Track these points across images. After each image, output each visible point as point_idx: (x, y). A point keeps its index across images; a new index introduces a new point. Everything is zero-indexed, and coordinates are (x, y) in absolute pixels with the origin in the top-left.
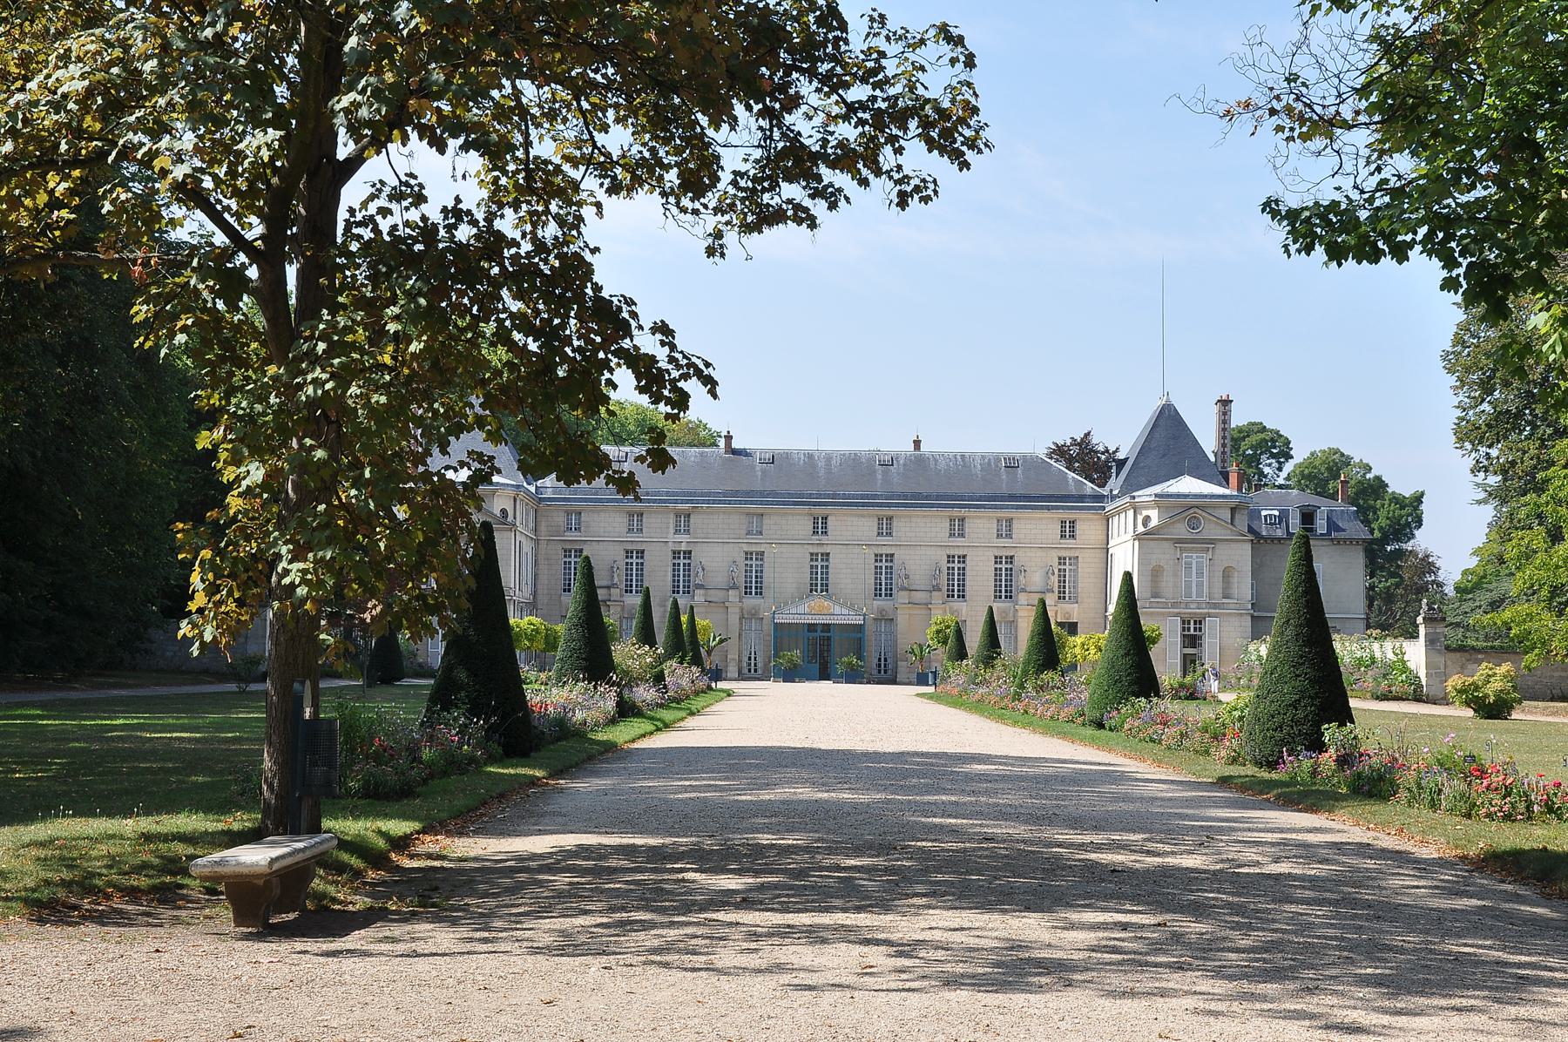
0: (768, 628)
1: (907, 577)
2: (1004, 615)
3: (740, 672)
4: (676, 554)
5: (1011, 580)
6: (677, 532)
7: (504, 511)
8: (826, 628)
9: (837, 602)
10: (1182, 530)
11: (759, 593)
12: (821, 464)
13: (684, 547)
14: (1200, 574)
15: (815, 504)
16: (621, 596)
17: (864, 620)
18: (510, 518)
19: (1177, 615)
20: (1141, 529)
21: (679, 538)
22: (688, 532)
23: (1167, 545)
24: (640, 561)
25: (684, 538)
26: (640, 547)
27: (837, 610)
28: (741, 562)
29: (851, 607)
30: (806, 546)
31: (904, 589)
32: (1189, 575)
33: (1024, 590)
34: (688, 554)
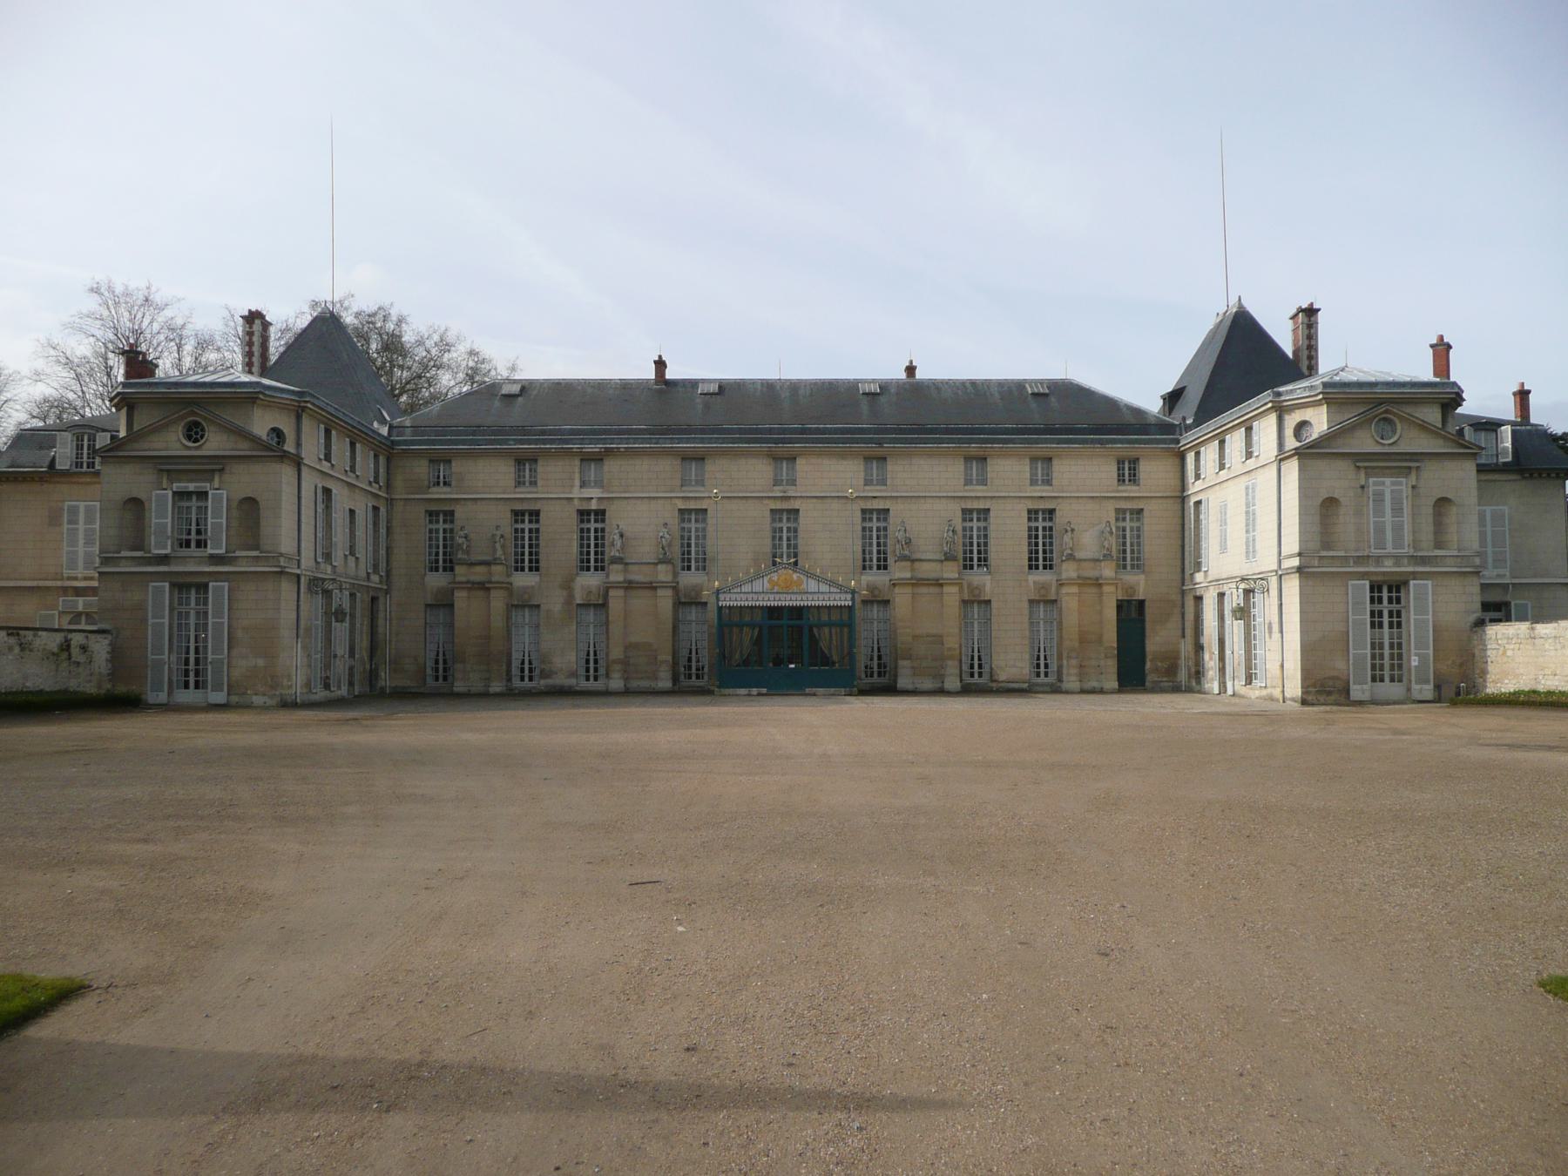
0: (712, 613)
1: (909, 542)
2: (1043, 592)
3: (675, 679)
4: (583, 514)
5: (1051, 544)
6: (583, 485)
7: (277, 433)
8: (798, 612)
9: (810, 575)
10: (1365, 442)
11: (703, 565)
12: (785, 394)
13: (594, 506)
14: (1397, 511)
15: (776, 441)
16: (509, 575)
17: (853, 599)
18: (289, 447)
19: (1363, 576)
20: (1291, 443)
21: (587, 493)
22: (599, 484)
23: (1343, 466)
24: (534, 526)
25: (594, 493)
26: (533, 507)
27: (812, 585)
28: (674, 521)
29: (832, 583)
30: (766, 502)
31: (904, 558)
32: (1379, 512)
33: (1071, 557)
34: (600, 514)
